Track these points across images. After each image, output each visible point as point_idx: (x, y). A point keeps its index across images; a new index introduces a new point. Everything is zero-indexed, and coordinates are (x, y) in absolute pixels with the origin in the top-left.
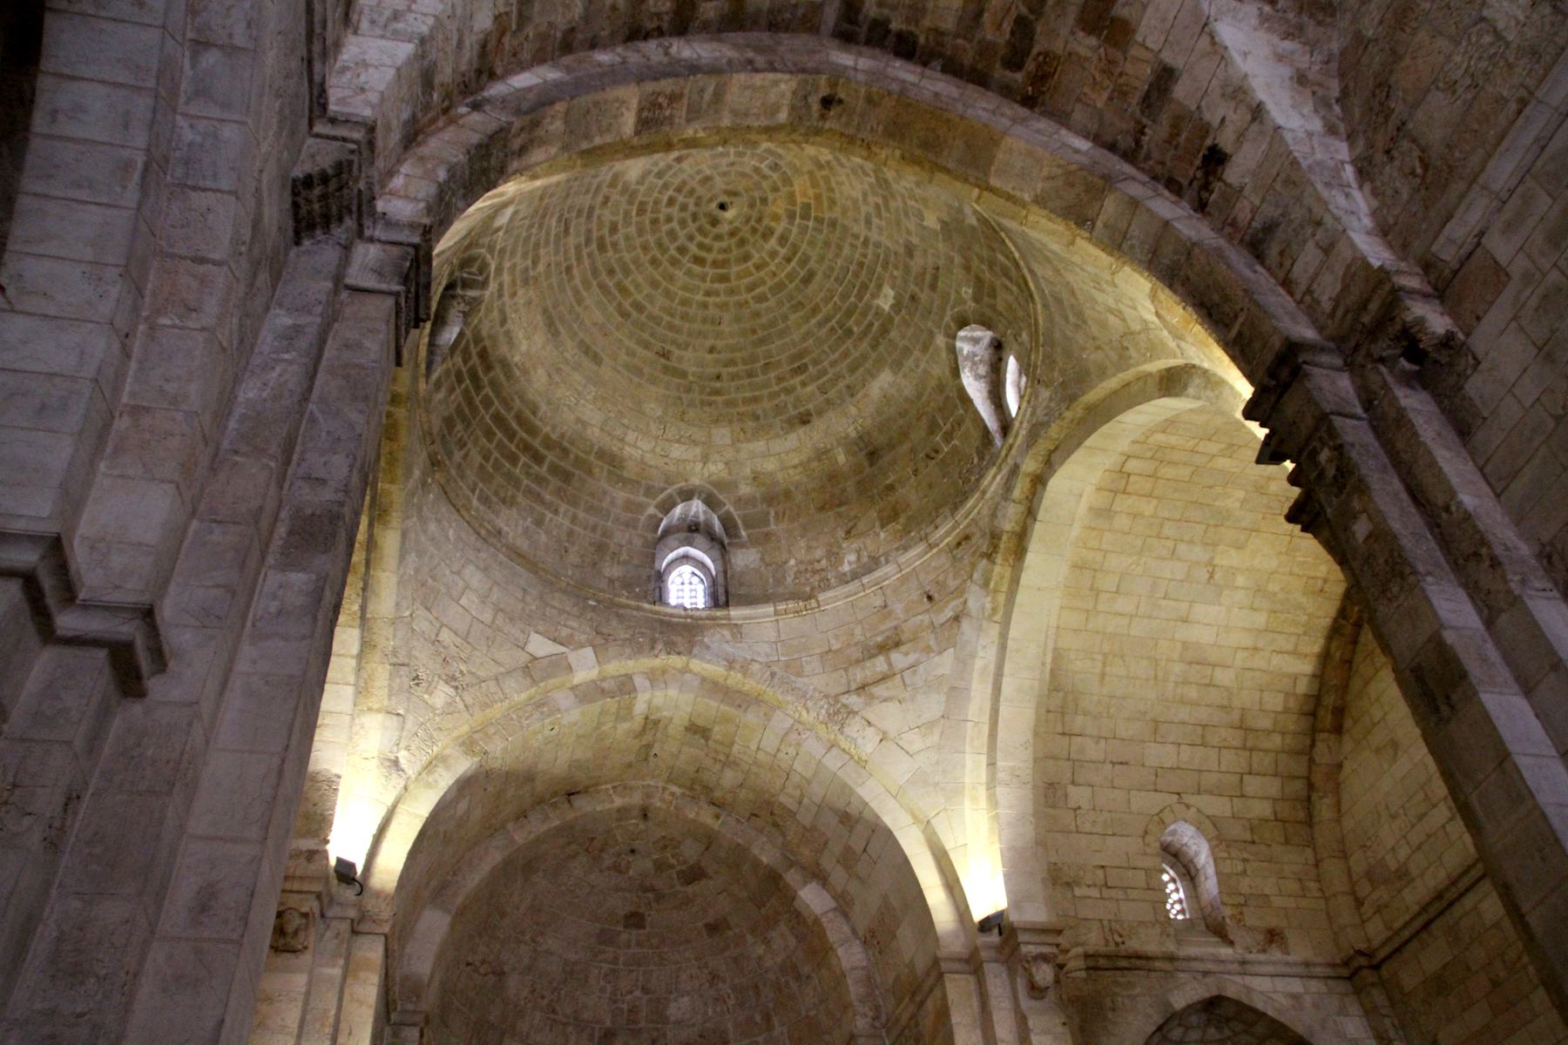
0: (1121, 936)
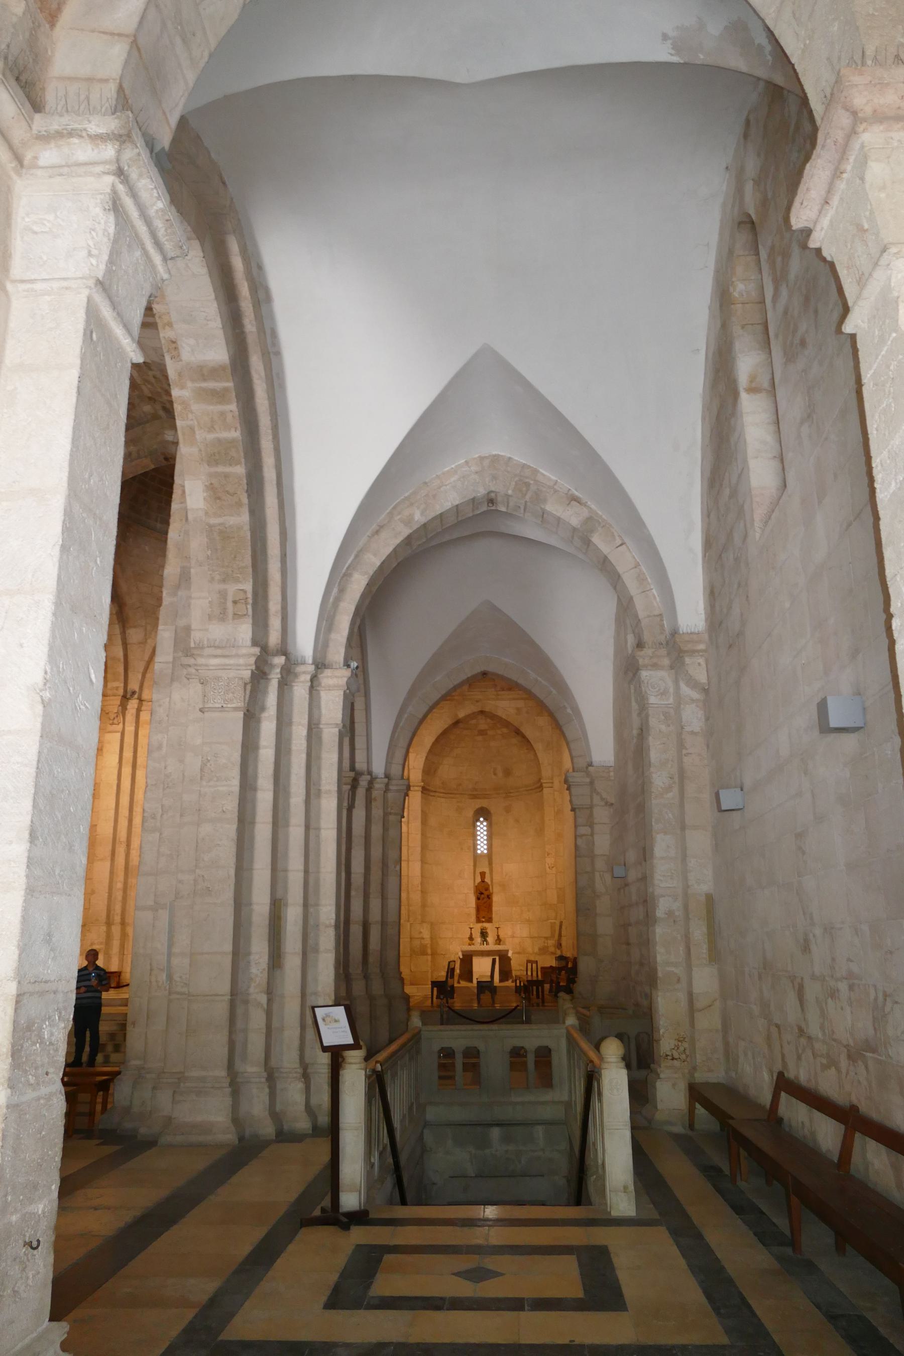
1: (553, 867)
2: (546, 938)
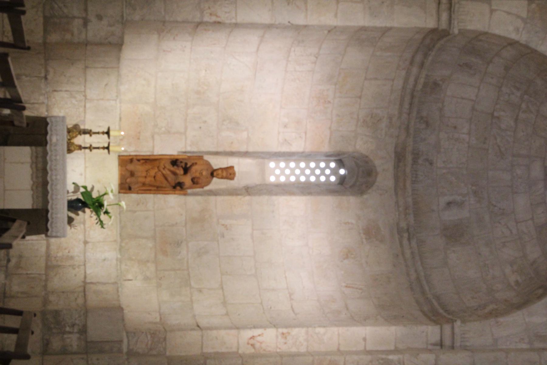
1: (253, 345)
2: (83, 331)
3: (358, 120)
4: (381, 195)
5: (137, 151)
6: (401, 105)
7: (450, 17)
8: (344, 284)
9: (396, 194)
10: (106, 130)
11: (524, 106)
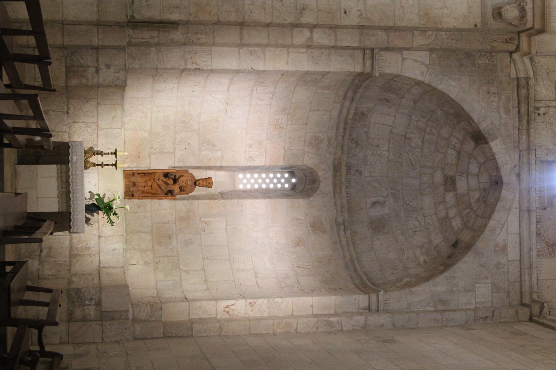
0: (544, 114)
2: (99, 303)
3: (305, 141)
4: (323, 197)
5: (138, 167)
6: (337, 129)
7: (373, 64)
8: (297, 265)
9: (335, 197)
10: (114, 152)
11: (428, 130)
